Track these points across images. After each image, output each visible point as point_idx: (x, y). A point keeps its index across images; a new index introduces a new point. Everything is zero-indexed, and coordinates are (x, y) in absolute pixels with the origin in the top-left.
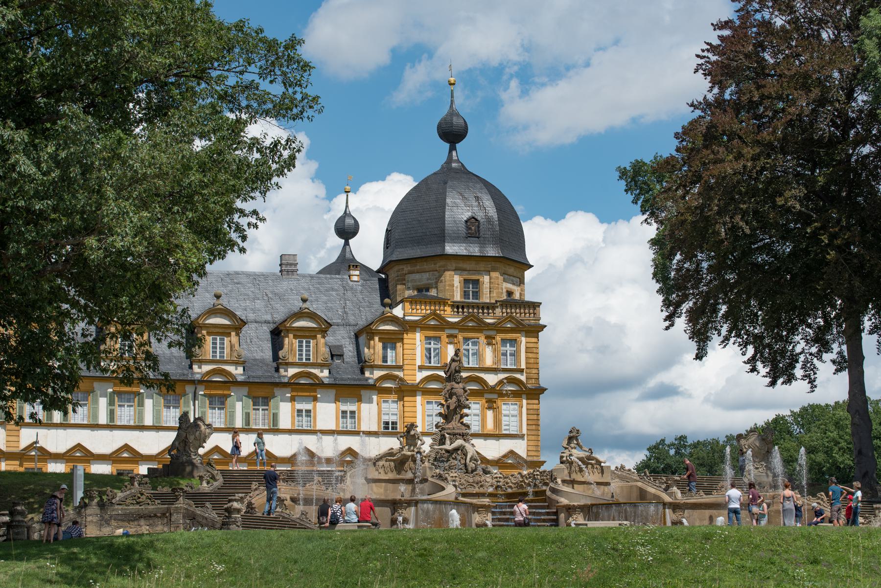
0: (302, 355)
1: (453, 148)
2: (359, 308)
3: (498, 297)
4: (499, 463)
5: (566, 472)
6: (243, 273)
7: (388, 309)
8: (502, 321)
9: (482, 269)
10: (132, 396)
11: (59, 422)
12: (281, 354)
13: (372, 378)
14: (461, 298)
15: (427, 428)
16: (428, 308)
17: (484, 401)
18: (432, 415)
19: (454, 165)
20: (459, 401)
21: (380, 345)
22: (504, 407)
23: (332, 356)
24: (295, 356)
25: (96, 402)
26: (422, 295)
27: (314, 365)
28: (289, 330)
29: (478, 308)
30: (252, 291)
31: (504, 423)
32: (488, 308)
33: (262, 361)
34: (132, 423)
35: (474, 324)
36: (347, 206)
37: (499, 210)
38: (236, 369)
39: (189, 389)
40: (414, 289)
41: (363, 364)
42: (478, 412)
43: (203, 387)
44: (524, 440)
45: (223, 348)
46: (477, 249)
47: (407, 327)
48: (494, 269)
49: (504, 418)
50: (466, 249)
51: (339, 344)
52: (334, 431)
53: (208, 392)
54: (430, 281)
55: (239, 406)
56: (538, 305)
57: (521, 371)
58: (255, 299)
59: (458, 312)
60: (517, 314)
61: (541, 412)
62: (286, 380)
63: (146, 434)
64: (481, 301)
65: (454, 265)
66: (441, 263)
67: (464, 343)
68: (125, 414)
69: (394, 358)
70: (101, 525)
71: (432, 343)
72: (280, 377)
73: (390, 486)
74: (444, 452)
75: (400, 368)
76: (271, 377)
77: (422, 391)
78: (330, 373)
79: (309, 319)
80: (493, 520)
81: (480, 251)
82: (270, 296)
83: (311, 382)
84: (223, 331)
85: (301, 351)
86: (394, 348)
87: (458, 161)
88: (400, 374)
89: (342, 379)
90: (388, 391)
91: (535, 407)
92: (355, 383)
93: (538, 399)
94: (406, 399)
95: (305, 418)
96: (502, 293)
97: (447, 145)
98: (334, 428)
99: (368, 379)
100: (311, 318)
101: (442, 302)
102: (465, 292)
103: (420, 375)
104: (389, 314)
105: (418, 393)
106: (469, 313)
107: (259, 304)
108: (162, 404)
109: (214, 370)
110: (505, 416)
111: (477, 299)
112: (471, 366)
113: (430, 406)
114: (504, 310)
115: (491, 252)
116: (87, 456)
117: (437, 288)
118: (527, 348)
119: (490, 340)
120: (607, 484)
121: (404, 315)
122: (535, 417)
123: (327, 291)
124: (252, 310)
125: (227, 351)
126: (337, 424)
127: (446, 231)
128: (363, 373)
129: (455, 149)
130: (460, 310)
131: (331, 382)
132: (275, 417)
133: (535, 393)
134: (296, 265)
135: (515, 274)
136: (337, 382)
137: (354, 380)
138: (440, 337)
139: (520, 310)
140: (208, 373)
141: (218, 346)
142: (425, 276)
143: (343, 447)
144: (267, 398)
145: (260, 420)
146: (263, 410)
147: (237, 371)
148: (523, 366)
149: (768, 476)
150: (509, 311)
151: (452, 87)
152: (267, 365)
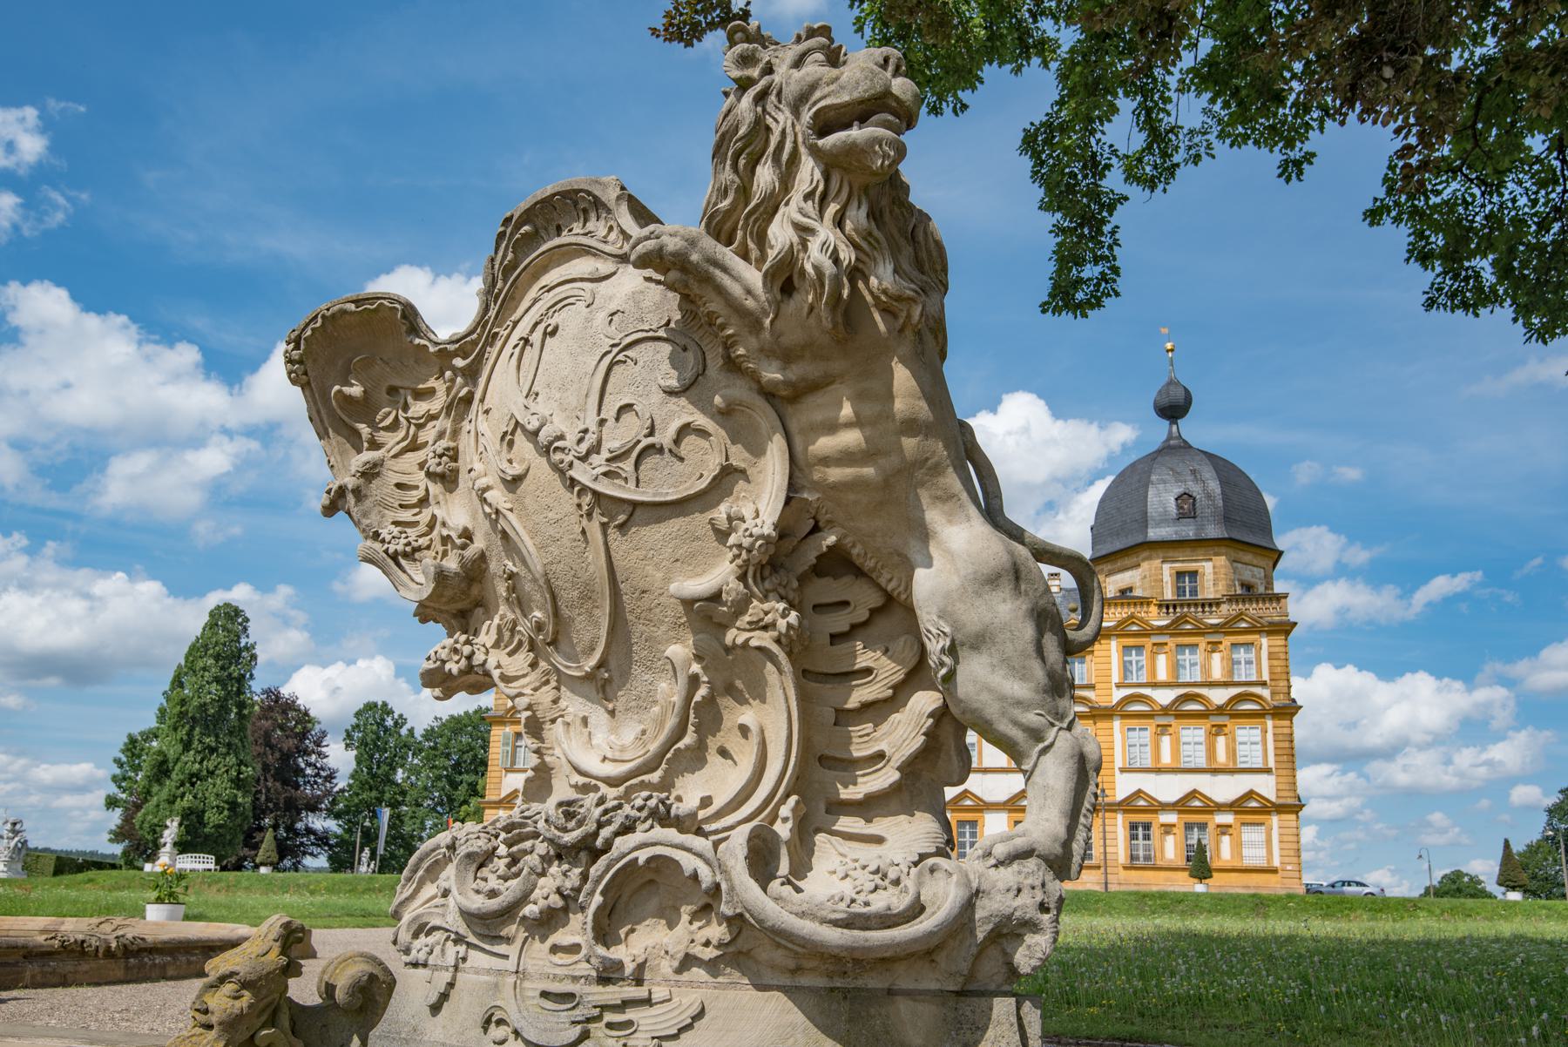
22: (1239, 732)
29: (1196, 605)
32: (1210, 605)
37: (1224, 483)
48: (1217, 554)
56: (1285, 596)
57: (1264, 684)
75: (1091, 687)
81: (1196, 534)
91: (1286, 731)
97: (1167, 423)
101: (1144, 602)
102: (1178, 588)
103: (1118, 695)
113: (1131, 734)
115: (1213, 531)
118: (1270, 653)
130: (1171, 610)
135: (1255, 562)
148: (1266, 677)
150: (1240, 606)
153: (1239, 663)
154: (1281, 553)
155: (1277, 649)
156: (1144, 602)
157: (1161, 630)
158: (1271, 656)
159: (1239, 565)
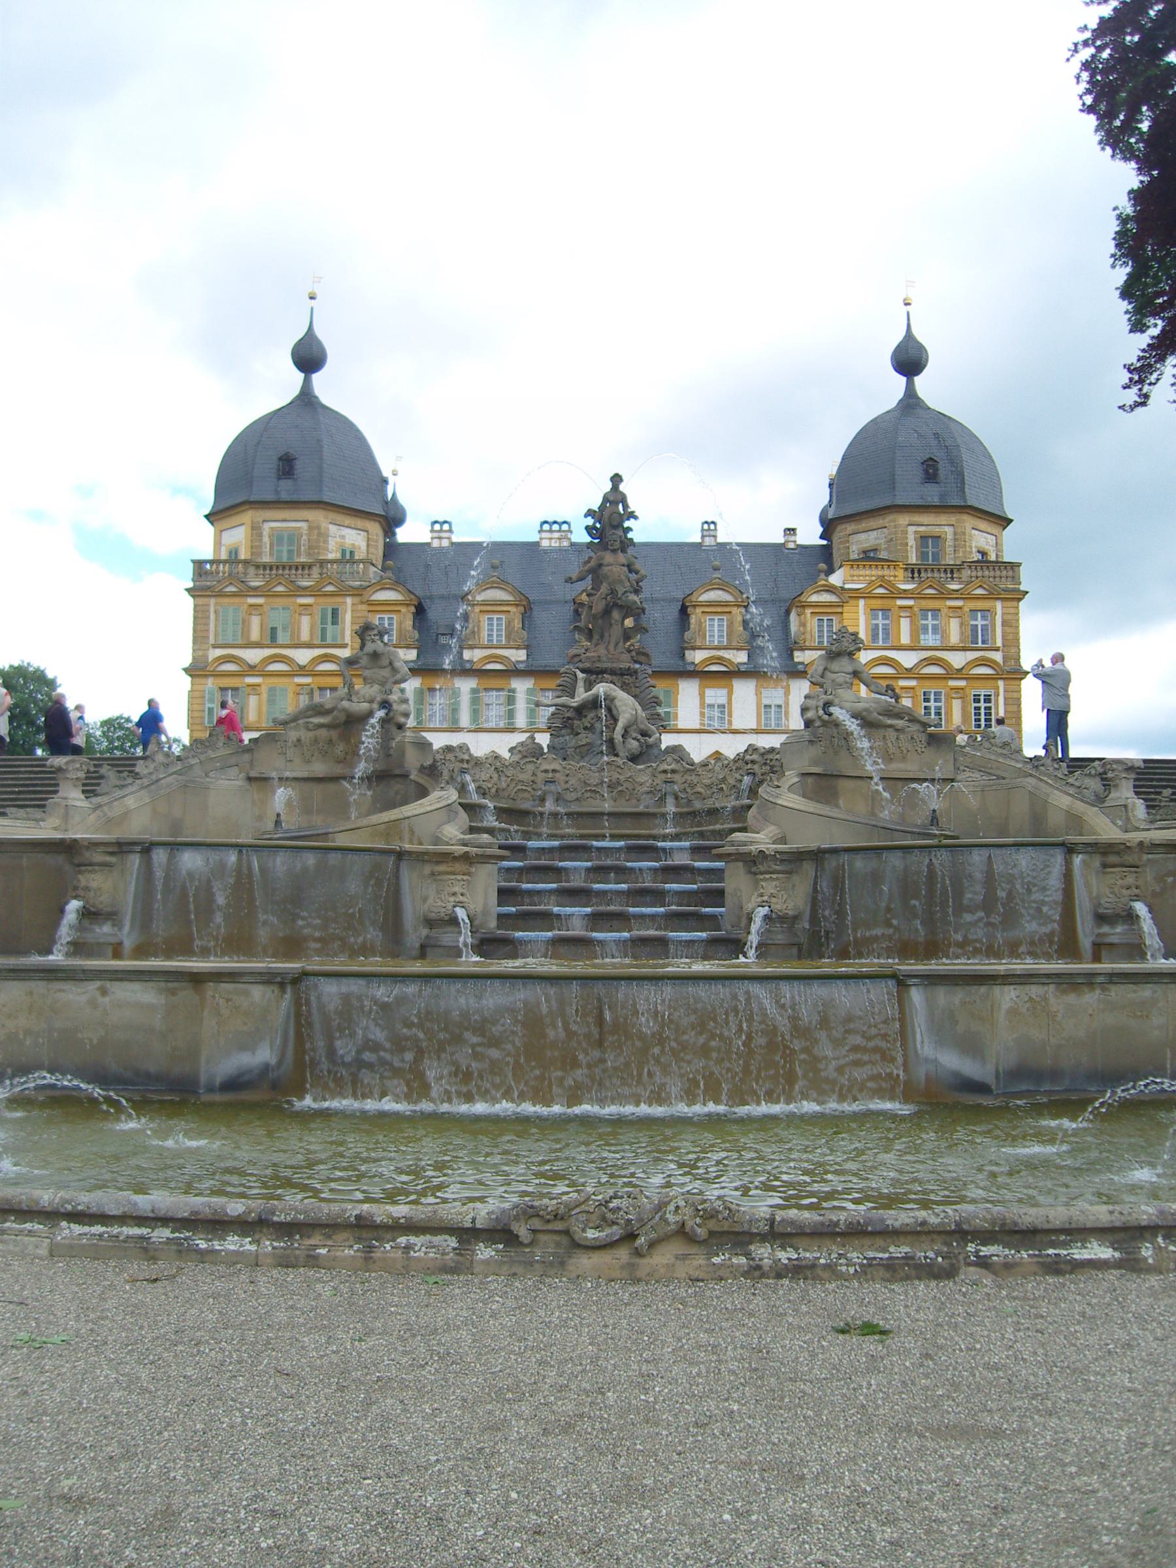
12: (687, 635)
13: (802, 663)
14: (917, 560)
47: (846, 596)
54: (878, 541)
56: (1019, 565)
59: (913, 578)
66: (891, 517)
91: (1015, 695)
98: (755, 727)
102: (922, 553)
104: (823, 582)
122: (1014, 708)
128: (791, 656)
130: (916, 575)
135: (989, 530)
142: (873, 534)
148: (999, 643)
154: (1010, 521)
155: (1010, 617)
156: (889, 563)
157: (905, 594)
158: (1004, 623)
159: (977, 532)
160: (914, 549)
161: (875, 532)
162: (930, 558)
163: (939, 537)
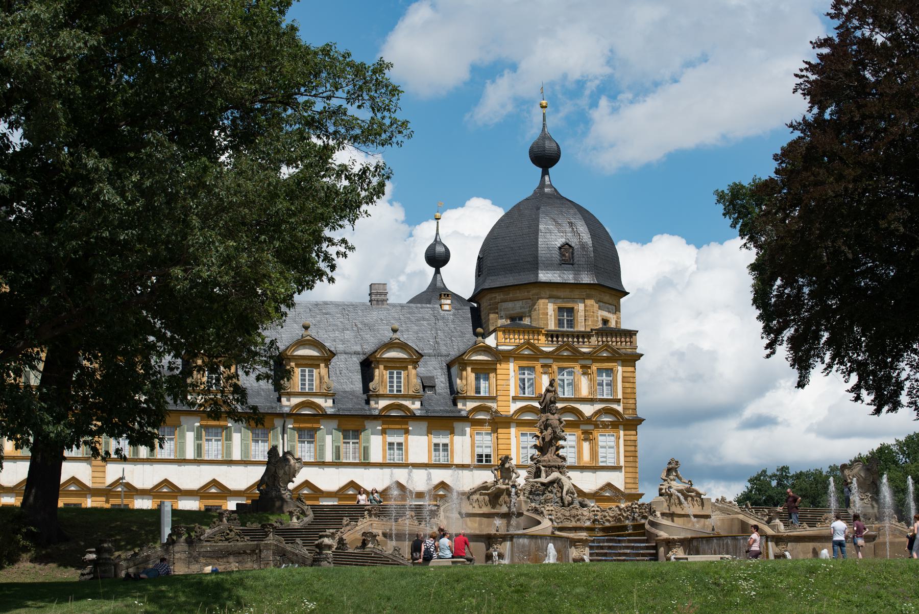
0: (392, 387)
1: (545, 173)
2: (451, 338)
3: (593, 325)
4: (596, 496)
5: (665, 504)
6: (332, 303)
7: (480, 338)
8: (597, 350)
9: (577, 297)
10: (220, 430)
11: (145, 457)
12: (372, 385)
13: (465, 410)
14: (555, 327)
15: (522, 460)
16: (521, 337)
17: (580, 432)
18: (526, 448)
19: (546, 190)
20: (554, 432)
21: (473, 375)
22: (600, 438)
23: (424, 387)
24: (386, 387)
25: (183, 437)
26: (515, 324)
27: (405, 397)
28: (379, 361)
29: (573, 337)
30: (341, 322)
31: (600, 455)
32: (583, 337)
33: (352, 393)
34: (220, 458)
35: (569, 354)
36: (437, 234)
37: (593, 236)
38: (326, 402)
39: (278, 422)
40: (507, 318)
41: (456, 396)
42: (574, 444)
43: (292, 421)
44: (621, 472)
45: (312, 380)
46: (571, 276)
48: (589, 297)
49: (600, 450)
50: (560, 277)
51: (430, 375)
52: (426, 464)
53: (297, 425)
54: (523, 310)
55: (329, 439)
58: (344, 329)
59: (552, 341)
60: (614, 342)
61: (639, 443)
62: (377, 413)
63: (234, 468)
64: (576, 329)
65: (547, 292)
66: (534, 291)
67: (559, 373)
68: (213, 449)
69: (487, 389)
70: (189, 562)
71: (526, 372)
72: (370, 410)
73: (485, 520)
74: (539, 485)
75: (493, 399)
76: (361, 409)
77: (517, 423)
78: (422, 405)
79: (399, 350)
80: (591, 554)
82: (360, 326)
83: (403, 414)
84: (312, 363)
85: (392, 382)
86: (487, 379)
87: (551, 186)
88: (493, 405)
89: (434, 411)
90: (481, 423)
91: (632, 438)
92: (448, 415)
93: (636, 430)
94: (500, 431)
95: (396, 452)
96: (598, 321)
97: (540, 170)
98: (426, 461)
99: (461, 410)
100: (402, 348)
101: (536, 331)
102: (559, 320)
104: (482, 344)
105: (512, 425)
106: (563, 342)
107: (348, 335)
108: (251, 438)
109: (303, 403)
110: (602, 447)
111: (571, 327)
112: (566, 396)
113: (524, 438)
114: (600, 339)
115: (586, 279)
116: (174, 492)
117: (530, 316)
119: (585, 370)
120: (708, 517)
121: (497, 345)
122: (632, 448)
123: (418, 320)
124: (341, 340)
125: (316, 383)
126: (430, 457)
127: (539, 258)
128: (455, 404)
129: (548, 174)
130: (555, 339)
131: (423, 415)
132: (366, 450)
133: (632, 424)
134: (386, 294)
135: (611, 302)
136: (429, 414)
137: (447, 411)
138: (534, 367)
139: (616, 338)
140: (297, 406)
141: (307, 378)
142: (519, 304)
143: (436, 481)
144: (358, 431)
145: (350, 452)
146: (353, 443)
147: (327, 404)
148: (620, 396)
149: (873, 507)
150: (604, 339)
151: (544, 110)
152: (358, 397)
153: (601, 384)
160: (553, 318)
161: (521, 302)
162: (565, 325)
163: (573, 308)
